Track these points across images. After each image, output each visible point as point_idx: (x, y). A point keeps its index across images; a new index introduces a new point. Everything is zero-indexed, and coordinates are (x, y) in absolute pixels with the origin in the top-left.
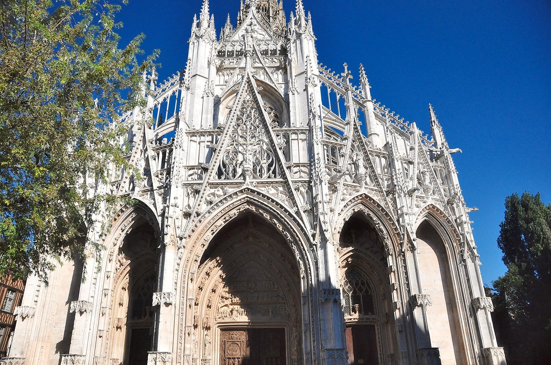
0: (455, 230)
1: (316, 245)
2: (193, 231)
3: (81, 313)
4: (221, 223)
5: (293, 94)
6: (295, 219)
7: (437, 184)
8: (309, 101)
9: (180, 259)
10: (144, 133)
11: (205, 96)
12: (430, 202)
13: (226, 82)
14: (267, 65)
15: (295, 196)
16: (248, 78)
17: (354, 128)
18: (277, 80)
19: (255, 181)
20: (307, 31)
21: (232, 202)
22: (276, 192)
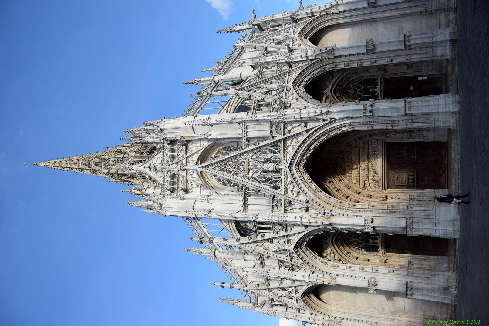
0: (318, 18)
2: (319, 205)
3: (376, 285)
4: (313, 186)
6: (312, 134)
7: (282, 30)
8: (221, 123)
9: (339, 214)
11: (210, 201)
12: (296, 36)
13: (198, 186)
14: (185, 155)
15: (295, 133)
16: (203, 167)
18: (196, 148)
19: (283, 162)
20: (158, 125)
22: (291, 147)
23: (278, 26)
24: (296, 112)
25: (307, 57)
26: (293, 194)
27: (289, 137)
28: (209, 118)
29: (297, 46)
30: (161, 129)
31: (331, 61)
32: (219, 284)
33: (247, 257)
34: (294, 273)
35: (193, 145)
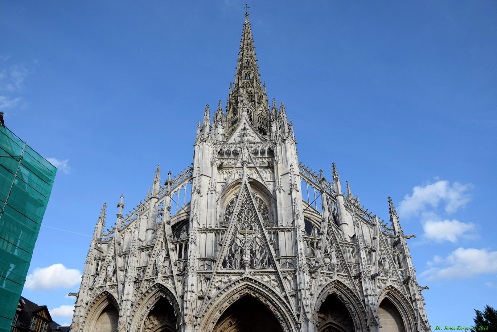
0: (410, 307)
1: (300, 324)
2: (206, 312)
4: (227, 305)
6: (283, 302)
7: (395, 267)
8: (293, 203)
10: (164, 228)
11: (209, 193)
12: (389, 283)
13: (226, 180)
14: (258, 165)
15: (284, 284)
16: (246, 185)
17: (328, 225)
18: (266, 177)
19: (252, 271)
20: (290, 137)
22: (269, 279)
23: (399, 263)
24: (306, 285)
25: (367, 296)
26: (217, 282)
27: (279, 277)
28: (298, 191)
29: (378, 284)
30: (285, 140)
31: (363, 323)
32: (121, 202)
33: (150, 232)
34: (132, 284)
35: (269, 175)
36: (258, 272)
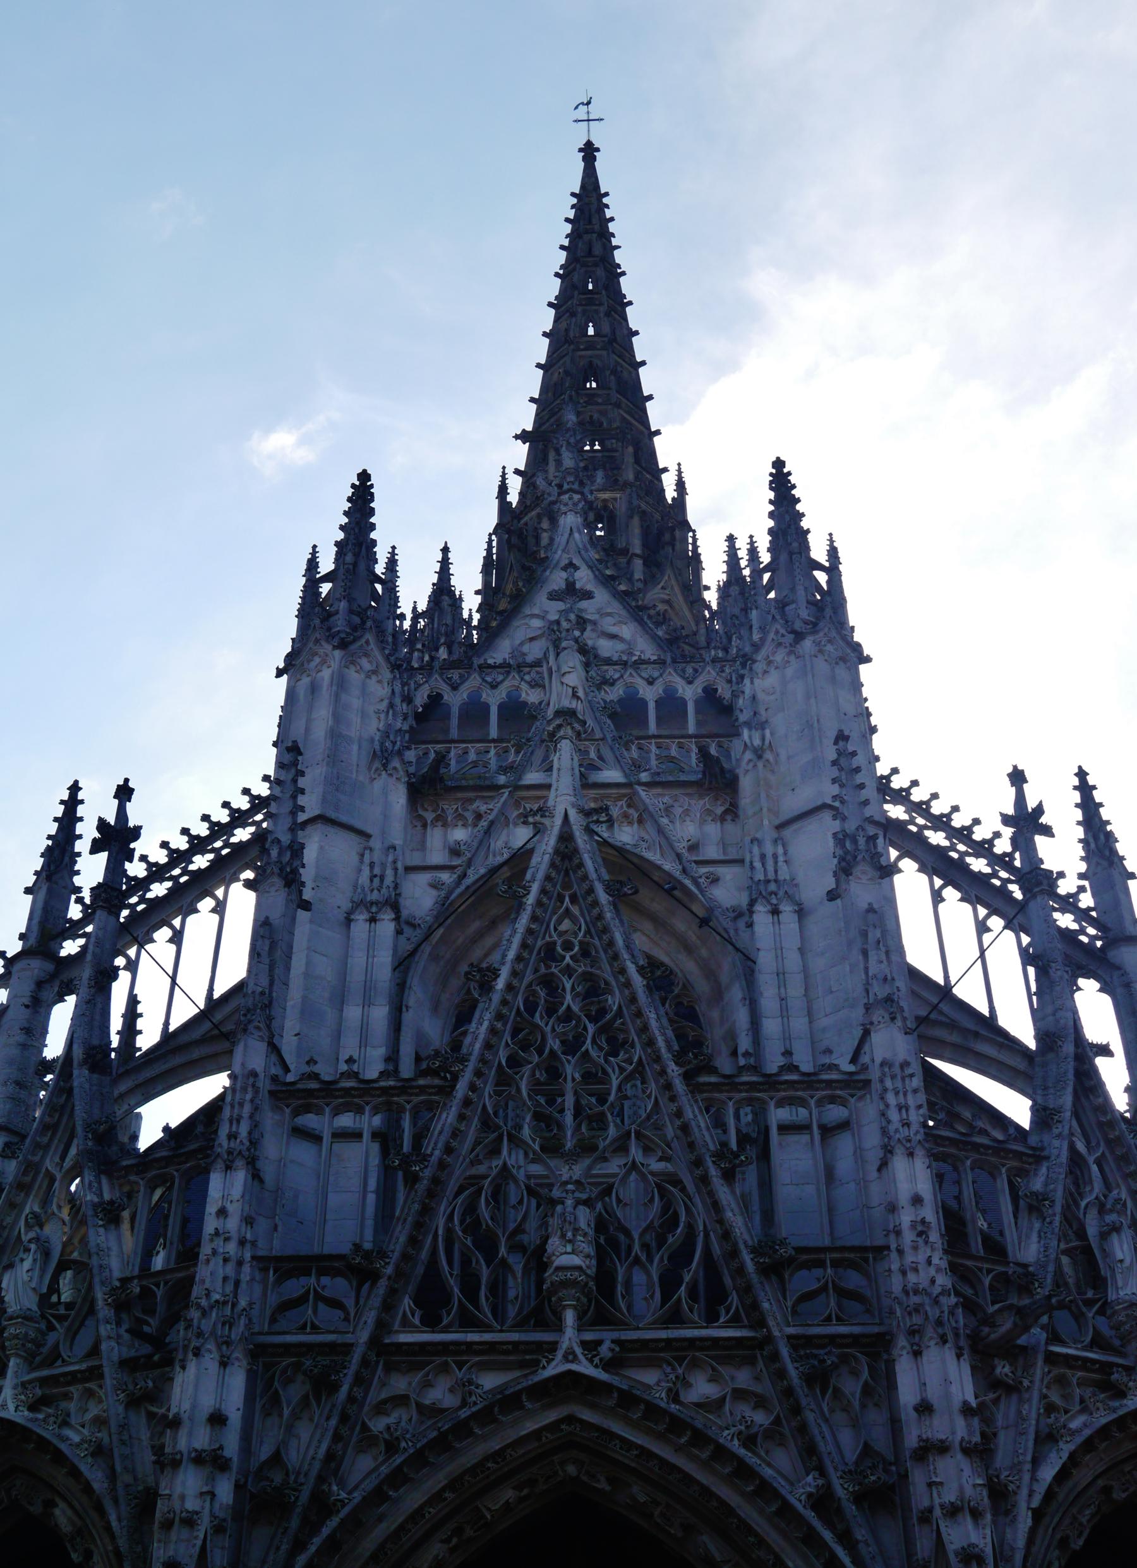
5: (775, 912)
6: (811, 1539)
11: (361, 917)
14: (644, 777)
15: (810, 1416)
19: (608, 1337)
21: (495, 1445)
27: (782, 1374)
36: (644, 1344)
